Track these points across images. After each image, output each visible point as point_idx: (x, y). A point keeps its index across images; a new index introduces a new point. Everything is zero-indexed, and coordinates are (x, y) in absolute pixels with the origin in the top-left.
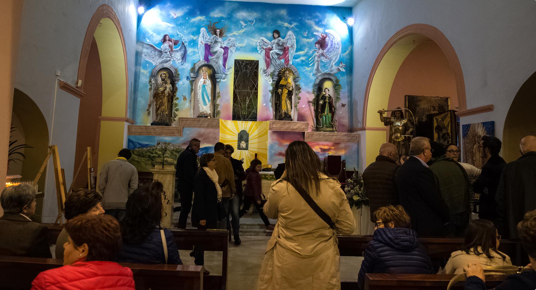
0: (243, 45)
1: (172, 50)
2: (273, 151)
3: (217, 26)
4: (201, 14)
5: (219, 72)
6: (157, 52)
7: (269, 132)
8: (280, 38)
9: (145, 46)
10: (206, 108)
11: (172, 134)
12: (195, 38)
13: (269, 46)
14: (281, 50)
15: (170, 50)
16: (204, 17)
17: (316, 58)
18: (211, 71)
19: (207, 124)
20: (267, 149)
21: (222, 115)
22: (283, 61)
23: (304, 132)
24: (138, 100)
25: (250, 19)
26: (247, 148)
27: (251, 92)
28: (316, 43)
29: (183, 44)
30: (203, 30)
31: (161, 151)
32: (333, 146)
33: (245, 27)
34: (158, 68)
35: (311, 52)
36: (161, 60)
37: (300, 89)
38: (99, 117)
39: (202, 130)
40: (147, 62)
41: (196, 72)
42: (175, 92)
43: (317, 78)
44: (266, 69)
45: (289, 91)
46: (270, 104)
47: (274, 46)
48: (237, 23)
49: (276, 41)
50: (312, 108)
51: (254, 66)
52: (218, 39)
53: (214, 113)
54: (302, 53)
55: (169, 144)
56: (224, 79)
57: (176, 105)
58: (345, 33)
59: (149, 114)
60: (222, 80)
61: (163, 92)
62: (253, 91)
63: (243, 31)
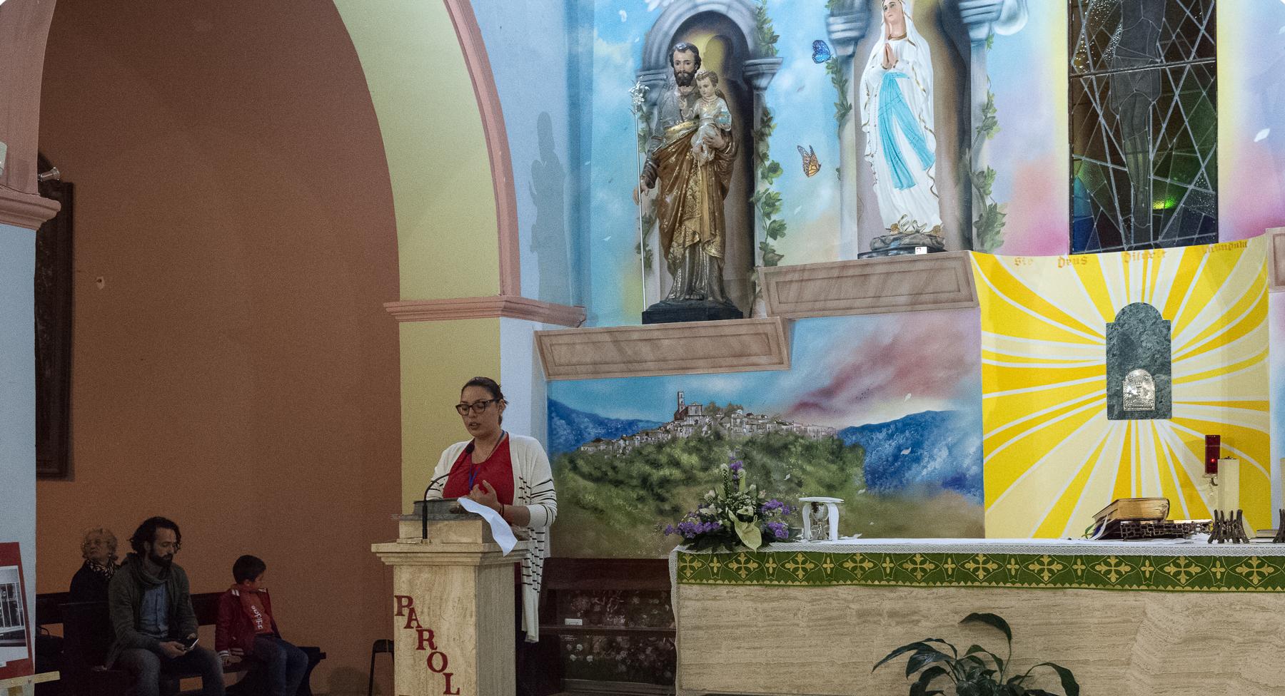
10: (918, 203)
11: (737, 359)
19: (905, 288)
20: (1264, 406)
21: (1009, 228)
24: (594, 203)
26: (1161, 409)
27: (1177, 73)
31: (697, 450)
34: (671, 24)
38: (390, 306)
39: (889, 327)
42: (762, 136)
53: (967, 223)
55: (731, 410)
56: (1012, 18)
57: (772, 203)
59: (648, 264)
60: (1000, 30)
61: (684, 145)
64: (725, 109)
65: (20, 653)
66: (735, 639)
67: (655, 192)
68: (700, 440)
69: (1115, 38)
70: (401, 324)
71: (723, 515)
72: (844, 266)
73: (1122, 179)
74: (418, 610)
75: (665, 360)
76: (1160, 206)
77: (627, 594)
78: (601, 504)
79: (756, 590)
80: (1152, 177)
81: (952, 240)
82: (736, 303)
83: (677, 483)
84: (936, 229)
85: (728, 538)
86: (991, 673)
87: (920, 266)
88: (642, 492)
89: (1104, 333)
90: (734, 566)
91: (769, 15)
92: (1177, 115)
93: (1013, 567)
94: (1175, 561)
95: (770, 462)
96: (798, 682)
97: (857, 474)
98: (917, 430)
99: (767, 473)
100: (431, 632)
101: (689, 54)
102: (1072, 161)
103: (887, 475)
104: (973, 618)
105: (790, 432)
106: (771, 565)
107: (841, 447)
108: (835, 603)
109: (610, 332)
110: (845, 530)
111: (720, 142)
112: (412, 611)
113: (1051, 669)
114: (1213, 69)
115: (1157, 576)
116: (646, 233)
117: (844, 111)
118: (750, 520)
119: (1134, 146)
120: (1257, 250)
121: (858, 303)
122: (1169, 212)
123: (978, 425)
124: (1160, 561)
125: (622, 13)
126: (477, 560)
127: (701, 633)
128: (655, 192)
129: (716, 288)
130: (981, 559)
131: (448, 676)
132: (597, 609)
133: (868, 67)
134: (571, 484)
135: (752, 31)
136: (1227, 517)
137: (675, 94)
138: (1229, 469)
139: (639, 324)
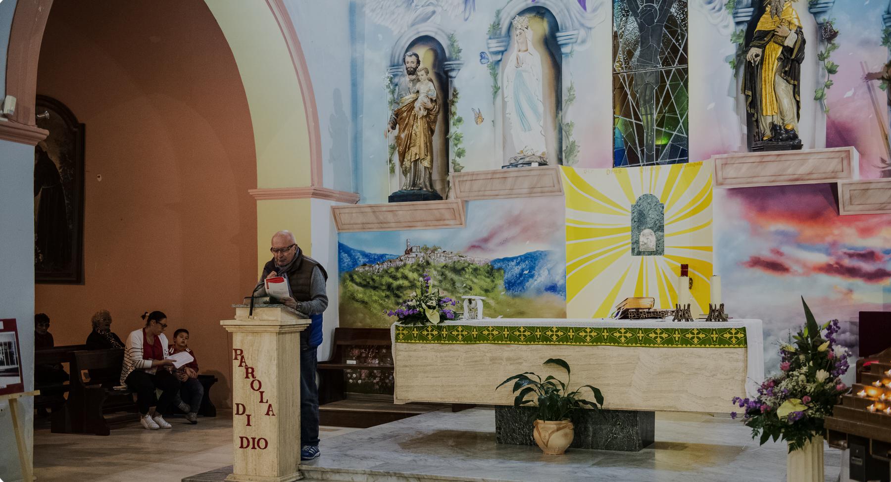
5: (568, 24)
7: (718, 193)
11: (439, 221)
18: (541, 27)
21: (581, 154)
23: (834, 186)
26: (659, 251)
27: (668, 73)
37: (834, 35)
39: (517, 205)
41: (503, 34)
42: (453, 102)
45: (788, 50)
46: (731, 101)
56: (583, 42)
57: (458, 139)
59: (392, 170)
60: (577, 48)
61: (411, 107)
64: (432, 88)
66: (425, 372)
68: (419, 265)
69: (637, 53)
70: (258, 202)
71: (420, 306)
72: (494, 173)
73: (640, 128)
74: (245, 357)
75: (400, 222)
76: (659, 143)
77: (379, 348)
78: (366, 299)
79: (436, 346)
80: (655, 127)
81: (552, 159)
82: (439, 192)
83: (406, 288)
84: (543, 154)
85: (422, 318)
86: (558, 391)
87: (533, 173)
88: (388, 293)
89: (630, 209)
90: (425, 333)
91: (457, 38)
95: (455, 277)
96: (458, 396)
97: (500, 283)
98: (532, 260)
99: (454, 283)
100: (253, 369)
101: (414, 57)
102: (614, 118)
104: (550, 361)
105: (465, 261)
106: (444, 333)
107: (492, 269)
108: (478, 353)
111: (430, 105)
112: (243, 357)
113: (589, 389)
114: (686, 71)
115: (645, 339)
116: (392, 154)
117: (496, 90)
118: (434, 308)
119: (646, 111)
120: (707, 167)
121: (502, 192)
122: (665, 145)
124: (647, 331)
125: (380, 35)
126: (277, 329)
127: (407, 369)
128: (396, 132)
129: (428, 184)
130: (555, 330)
131: (262, 393)
132: (364, 355)
133: (508, 66)
134: (350, 288)
135: (448, 46)
136: (682, 308)
137: (406, 80)
139: (386, 202)
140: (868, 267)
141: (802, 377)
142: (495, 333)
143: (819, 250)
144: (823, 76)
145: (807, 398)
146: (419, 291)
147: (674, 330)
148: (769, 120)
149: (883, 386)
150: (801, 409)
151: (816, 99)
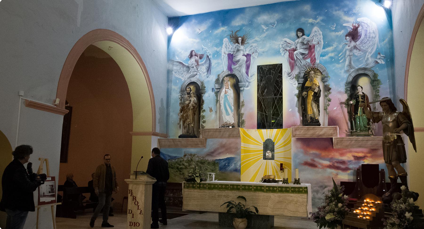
0: (266, 49)
1: (198, 64)
2: (298, 161)
3: (239, 34)
4: (224, 25)
5: (243, 80)
6: (185, 68)
7: (293, 139)
8: (304, 37)
9: (175, 63)
10: (230, 118)
11: (196, 145)
12: (218, 50)
13: (293, 47)
14: (306, 49)
15: (196, 64)
16: (226, 27)
17: (348, 53)
18: (233, 81)
19: (228, 134)
20: (291, 158)
21: (246, 124)
22: (309, 60)
25: (272, 21)
26: (273, 158)
27: (276, 98)
28: (346, 36)
29: (208, 57)
30: (226, 40)
32: (369, 153)
33: (267, 30)
34: (186, 83)
35: (341, 46)
36: (189, 75)
37: (330, 89)
39: (224, 141)
40: (177, 79)
41: (220, 82)
42: (202, 105)
43: (350, 75)
44: (290, 71)
45: (315, 93)
46: (297, 109)
47: (298, 46)
48: (258, 28)
49: (300, 40)
50: (346, 110)
51: (278, 69)
52: (240, 47)
54: (330, 49)
55: (194, 155)
56: (248, 86)
58: (382, 17)
60: (245, 88)
61: (188, 105)
62: (278, 96)
63: (264, 35)
65: (53, 199)
67: (182, 114)
68: (188, 160)
69: (265, 91)
70: (133, 137)
72: (217, 129)
73: (266, 116)
76: (273, 121)
79: (198, 190)
81: (236, 125)
87: (230, 130)
92: (276, 106)
93: (247, 187)
94: (276, 187)
97: (218, 168)
98: (229, 160)
101: (189, 89)
103: (223, 168)
105: (205, 160)
106: (202, 186)
107: (215, 163)
109: (172, 139)
110: (215, 180)
111: (194, 105)
114: (282, 98)
116: (180, 121)
117: (217, 101)
118: (198, 177)
120: (290, 130)
122: (274, 122)
123: (240, 160)
124: (273, 187)
128: (182, 114)
131: (138, 206)
138: (286, 171)
140: (343, 166)
141: (333, 206)
142: (220, 186)
143: (327, 160)
144: (327, 102)
145: (335, 213)
146: (192, 170)
147: (283, 187)
148: (310, 116)
149: (362, 209)
150: (333, 217)
151: (324, 109)
